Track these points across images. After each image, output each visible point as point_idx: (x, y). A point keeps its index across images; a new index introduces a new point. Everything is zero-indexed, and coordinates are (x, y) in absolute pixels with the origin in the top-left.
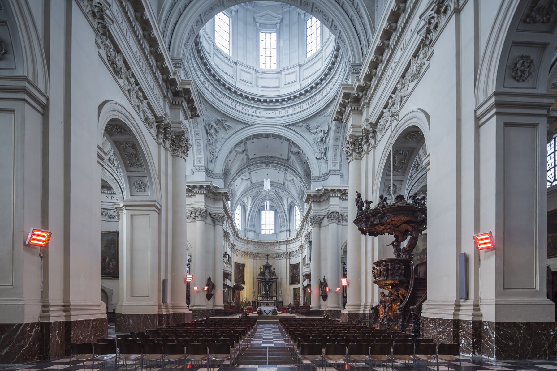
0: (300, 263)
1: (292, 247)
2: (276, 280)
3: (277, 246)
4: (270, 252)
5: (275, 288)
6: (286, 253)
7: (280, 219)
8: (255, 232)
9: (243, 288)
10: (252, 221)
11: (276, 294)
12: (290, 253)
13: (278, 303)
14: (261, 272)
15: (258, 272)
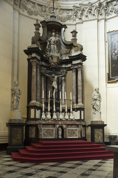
6: (97, 4)
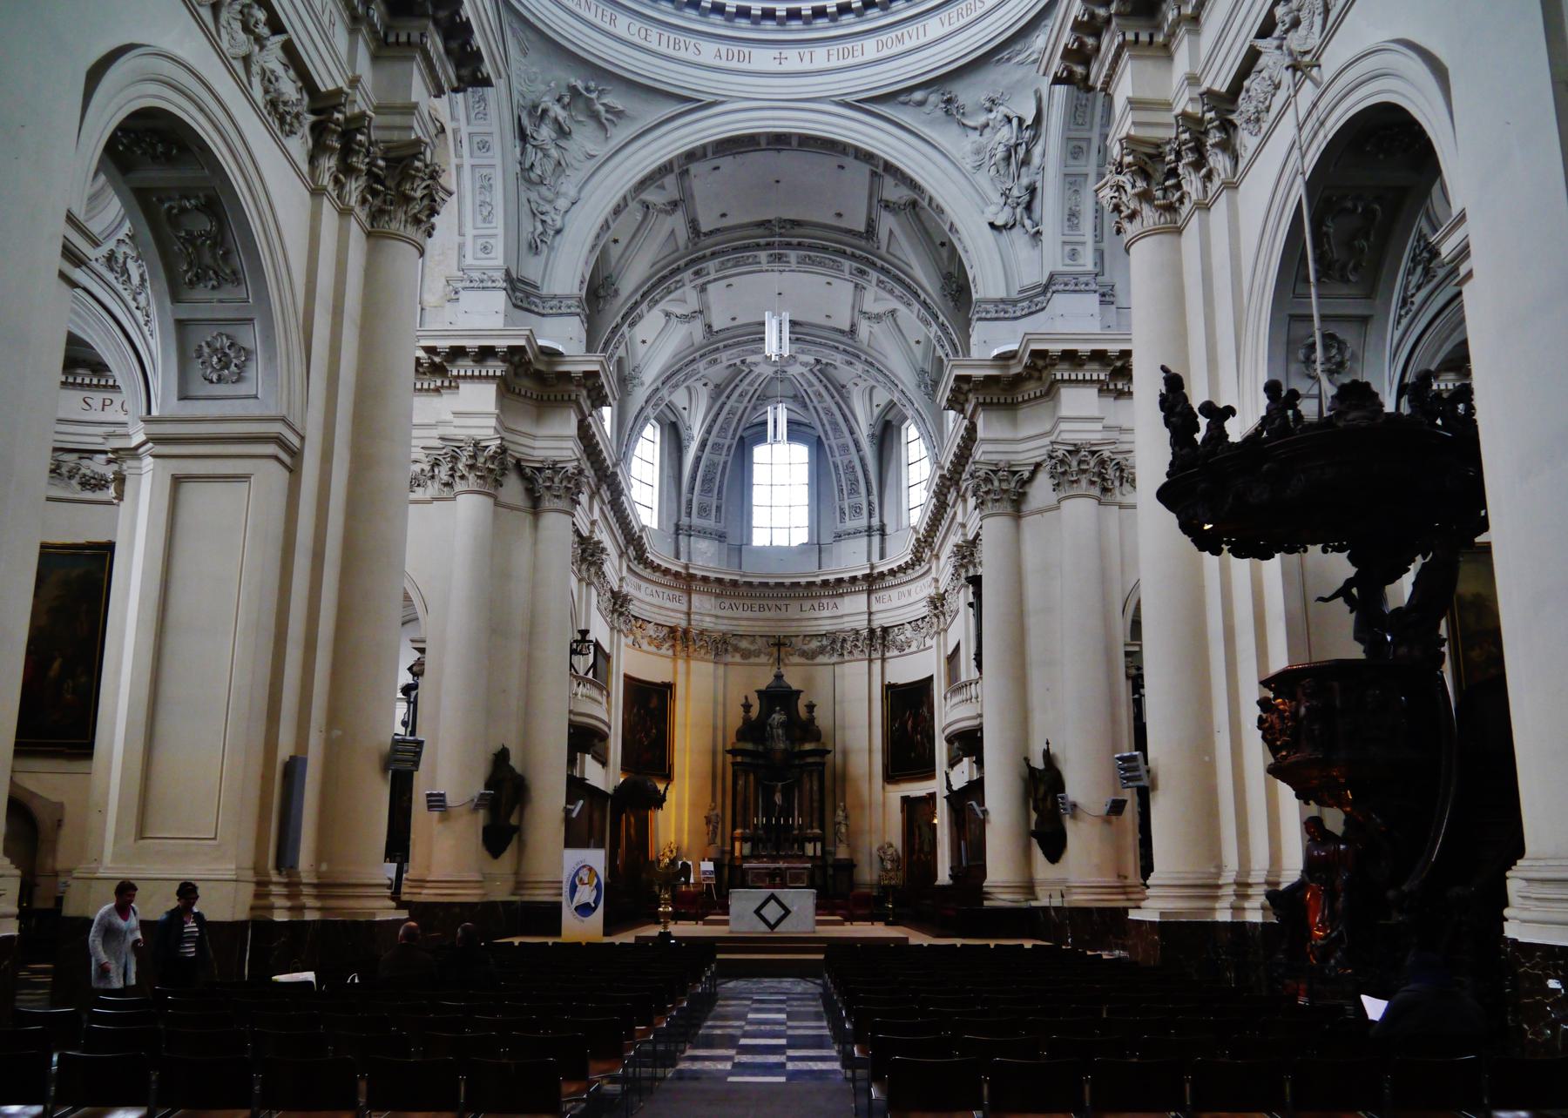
0: (932, 676)
1: (895, 603)
2: (817, 759)
3: (825, 601)
4: (793, 629)
5: (816, 797)
6: (865, 633)
7: (839, 481)
8: (721, 537)
9: (663, 799)
10: (710, 491)
11: (822, 827)
12: (885, 630)
13: (830, 871)
14: (747, 720)
15: (736, 720)
